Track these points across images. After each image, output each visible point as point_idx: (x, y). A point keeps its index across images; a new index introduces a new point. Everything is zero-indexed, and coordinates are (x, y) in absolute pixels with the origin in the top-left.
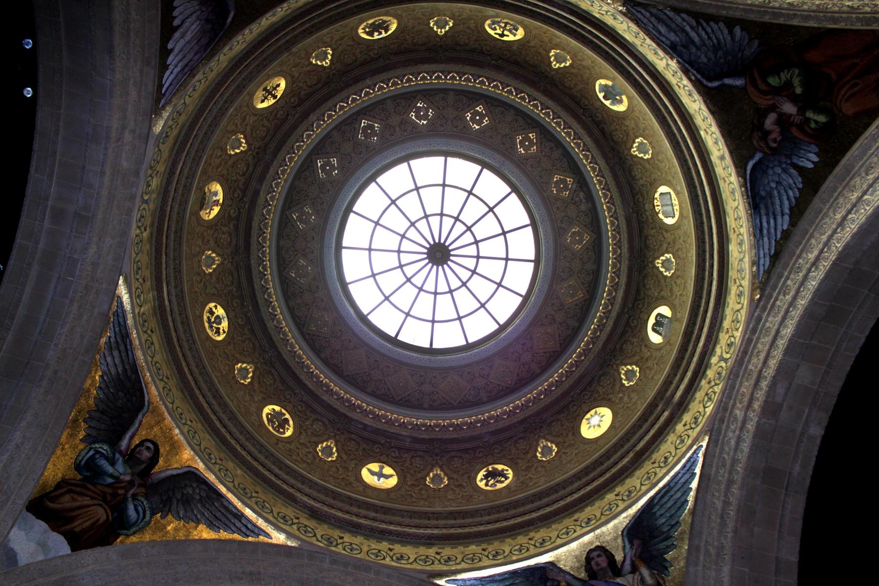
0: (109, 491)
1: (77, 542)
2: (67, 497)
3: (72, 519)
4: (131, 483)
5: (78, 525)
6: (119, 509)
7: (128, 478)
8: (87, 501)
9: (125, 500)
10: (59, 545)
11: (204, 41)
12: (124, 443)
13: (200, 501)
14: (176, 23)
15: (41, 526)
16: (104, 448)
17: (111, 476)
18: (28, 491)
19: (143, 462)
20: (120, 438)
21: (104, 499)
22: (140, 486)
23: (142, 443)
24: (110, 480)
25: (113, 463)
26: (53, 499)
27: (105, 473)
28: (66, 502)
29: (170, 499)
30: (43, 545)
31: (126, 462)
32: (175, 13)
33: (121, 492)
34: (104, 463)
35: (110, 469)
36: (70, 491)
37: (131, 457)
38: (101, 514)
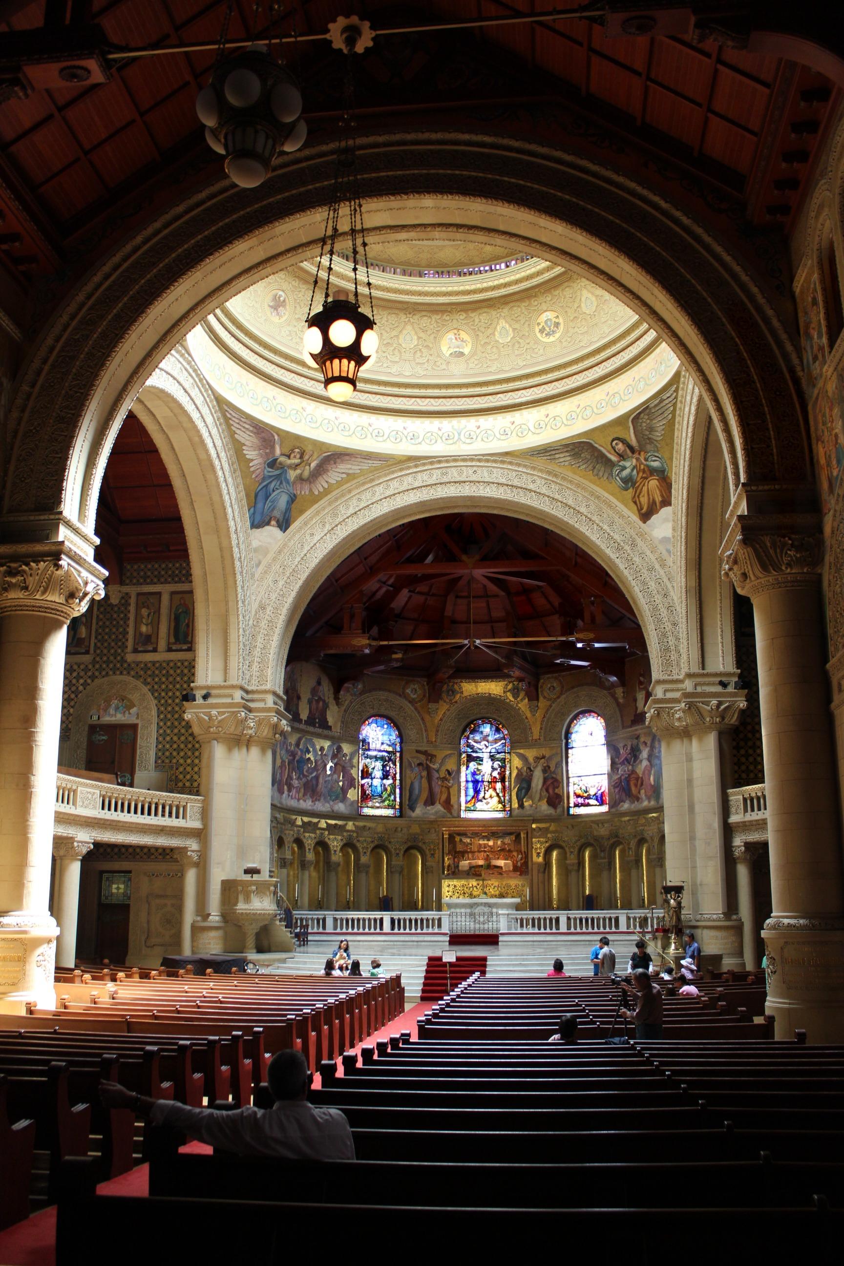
0: (641, 474)
1: (666, 502)
2: (642, 499)
3: (654, 502)
4: (637, 459)
5: (658, 499)
6: (652, 471)
7: (634, 461)
8: (645, 488)
9: (648, 466)
10: (665, 511)
11: (347, 458)
12: (614, 458)
13: (652, 420)
14: (344, 476)
15: (654, 518)
16: (616, 470)
17: (632, 470)
18: (635, 518)
19: (625, 451)
20: (609, 460)
21: (646, 478)
22: (639, 454)
23: (613, 448)
24: (635, 472)
25: (624, 468)
26: (642, 509)
27: (630, 475)
28: (644, 500)
29: (649, 439)
30: (666, 520)
31: (624, 460)
32: (340, 479)
33: (642, 467)
34: (625, 473)
35: (628, 471)
36: (638, 497)
37: (622, 456)
38: (653, 483)
